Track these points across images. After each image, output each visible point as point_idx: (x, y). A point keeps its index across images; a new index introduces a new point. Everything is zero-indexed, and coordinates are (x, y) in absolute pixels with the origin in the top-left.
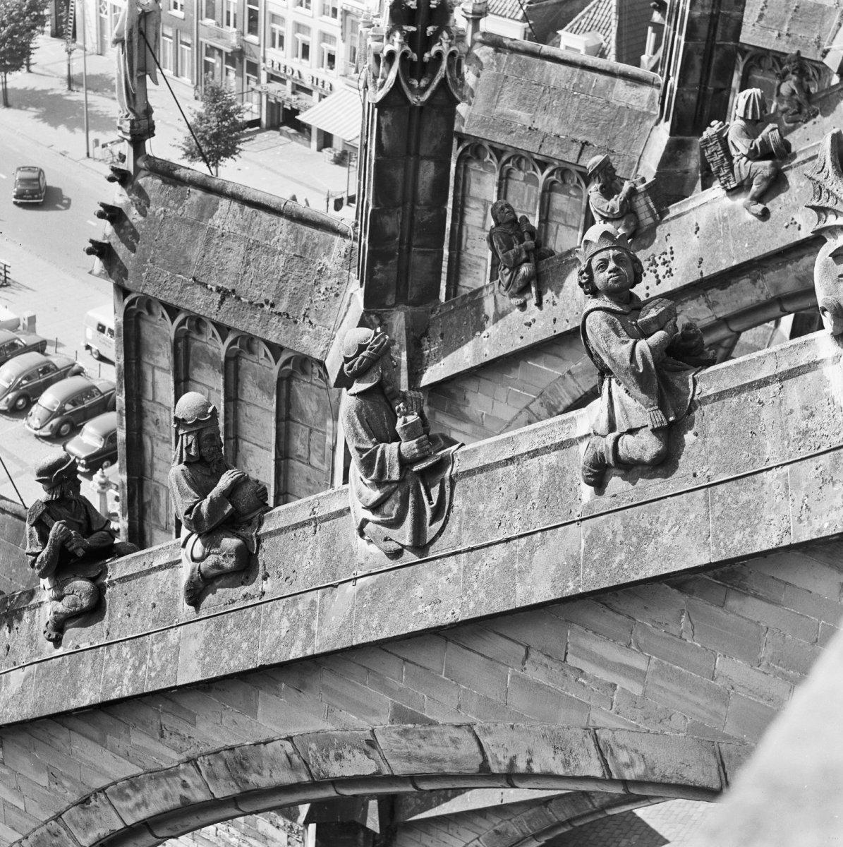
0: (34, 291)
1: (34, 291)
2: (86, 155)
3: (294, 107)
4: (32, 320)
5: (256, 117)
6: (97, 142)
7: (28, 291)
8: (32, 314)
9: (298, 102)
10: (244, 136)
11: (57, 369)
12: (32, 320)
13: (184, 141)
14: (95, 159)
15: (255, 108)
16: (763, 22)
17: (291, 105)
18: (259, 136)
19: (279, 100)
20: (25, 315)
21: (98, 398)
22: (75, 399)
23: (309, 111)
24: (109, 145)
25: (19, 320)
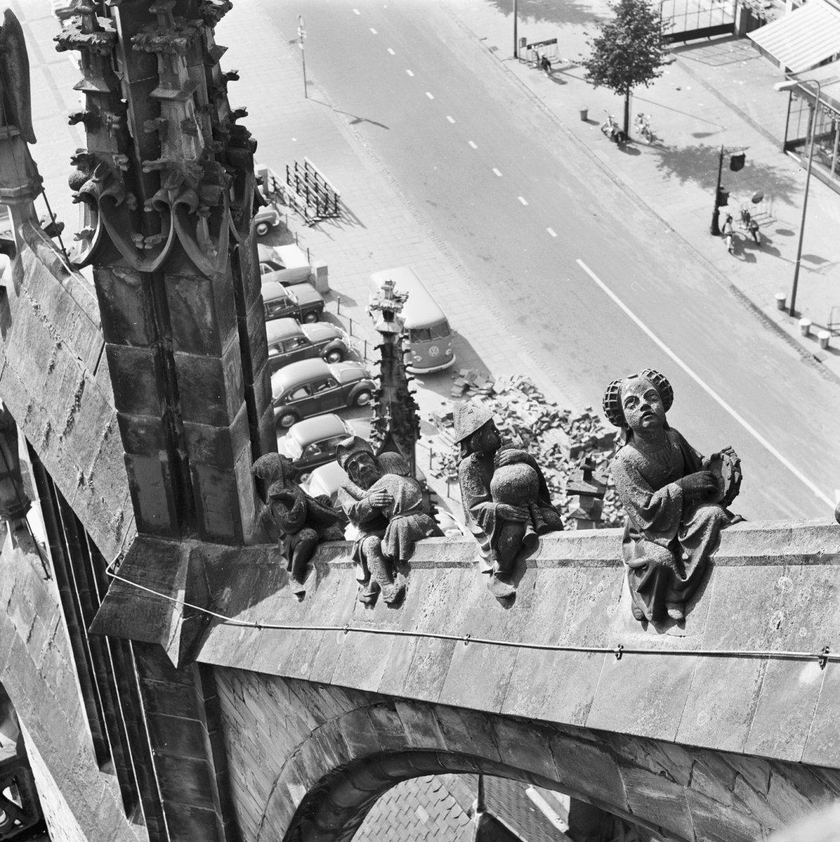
0: (363, 226)
1: (363, 226)
2: (513, 55)
3: (762, 17)
4: (323, 271)
5: (728, 21)
6: (524, 40)
7: (358, 226)
8: (324, 265)
9: (765, 11)
10: (667, 53)
11: (310, 343)
12: (323, 271)
13: (592, 57)
14: (520, 59)
15: (730, 10)
16: (70, 439)
17: (758, 14)
18: (729, 45)
19: (748, 6)
20: (316, 264)
21: (334, 389)
22: (312, 384)
23: (774, 23)
24: (533, 47)
25: (309, 269)
